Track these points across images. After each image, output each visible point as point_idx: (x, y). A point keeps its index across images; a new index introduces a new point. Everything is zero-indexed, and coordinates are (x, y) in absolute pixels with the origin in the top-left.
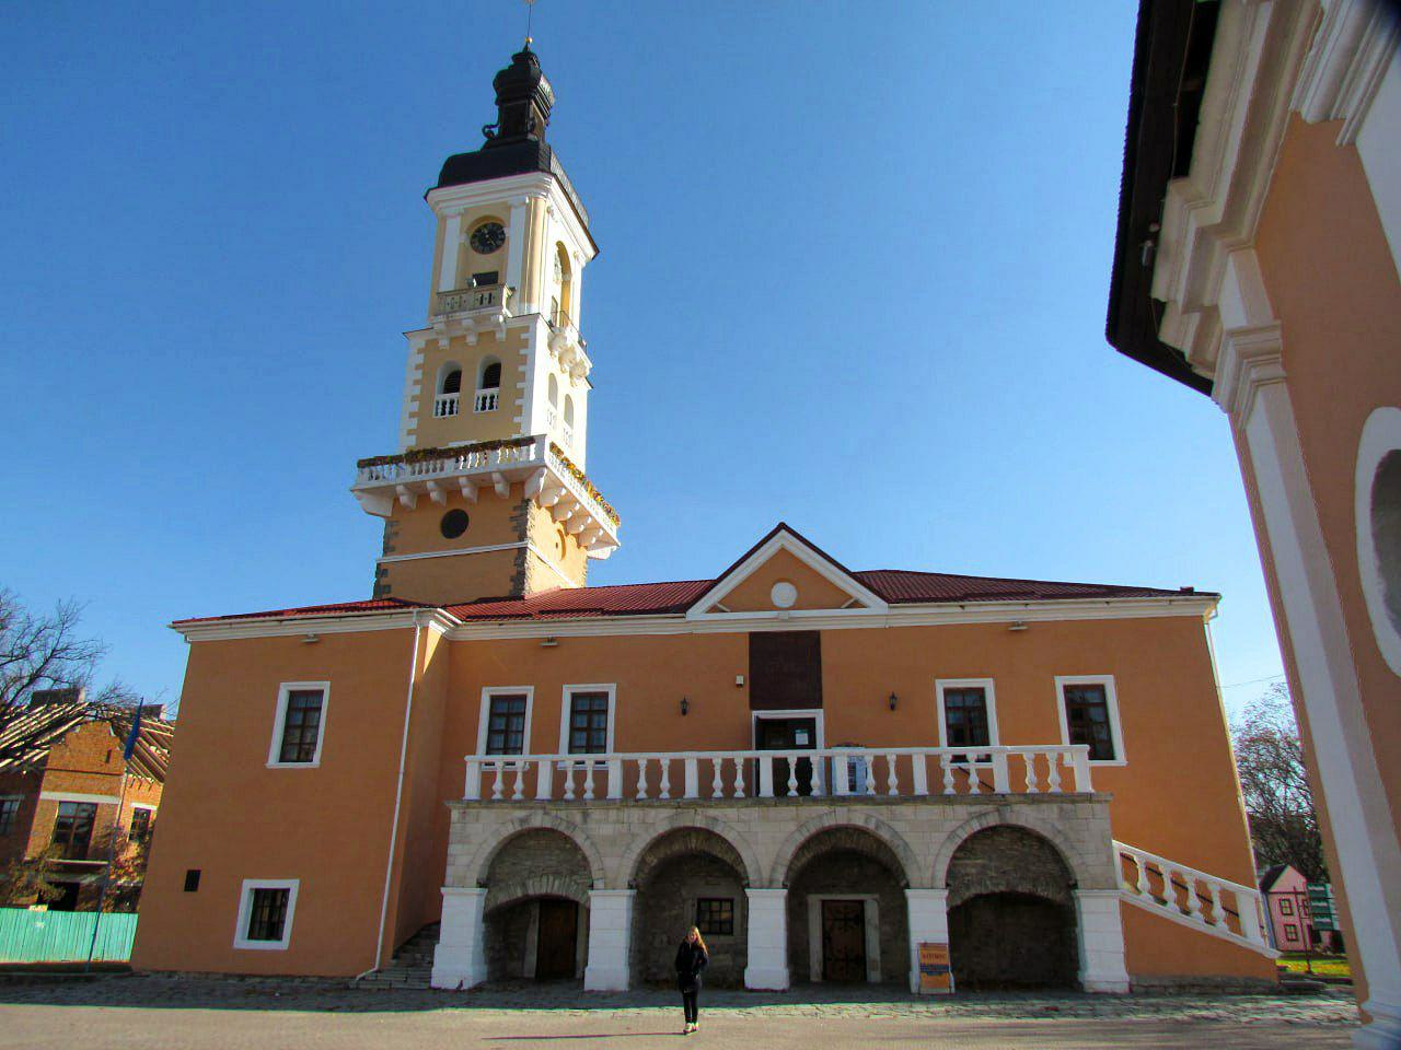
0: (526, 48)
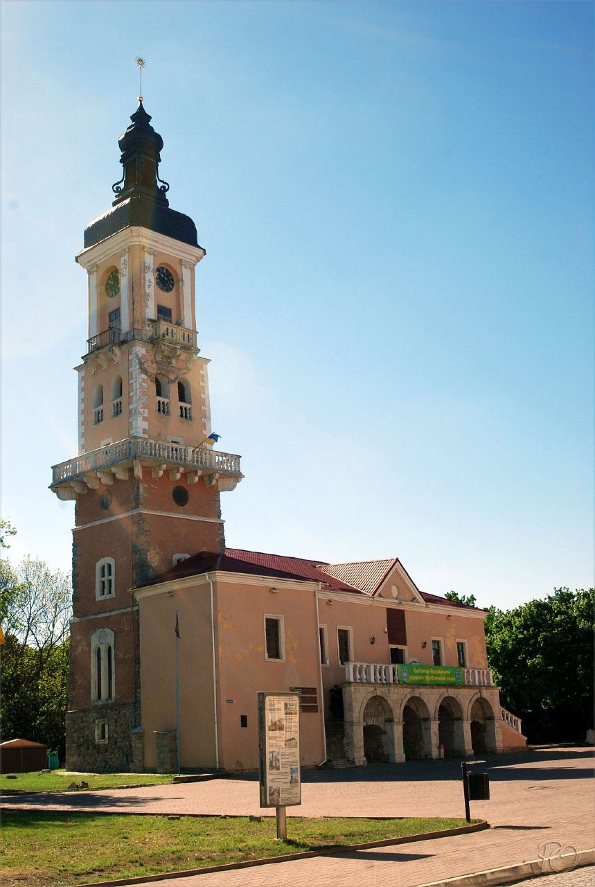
0: (141, 108)
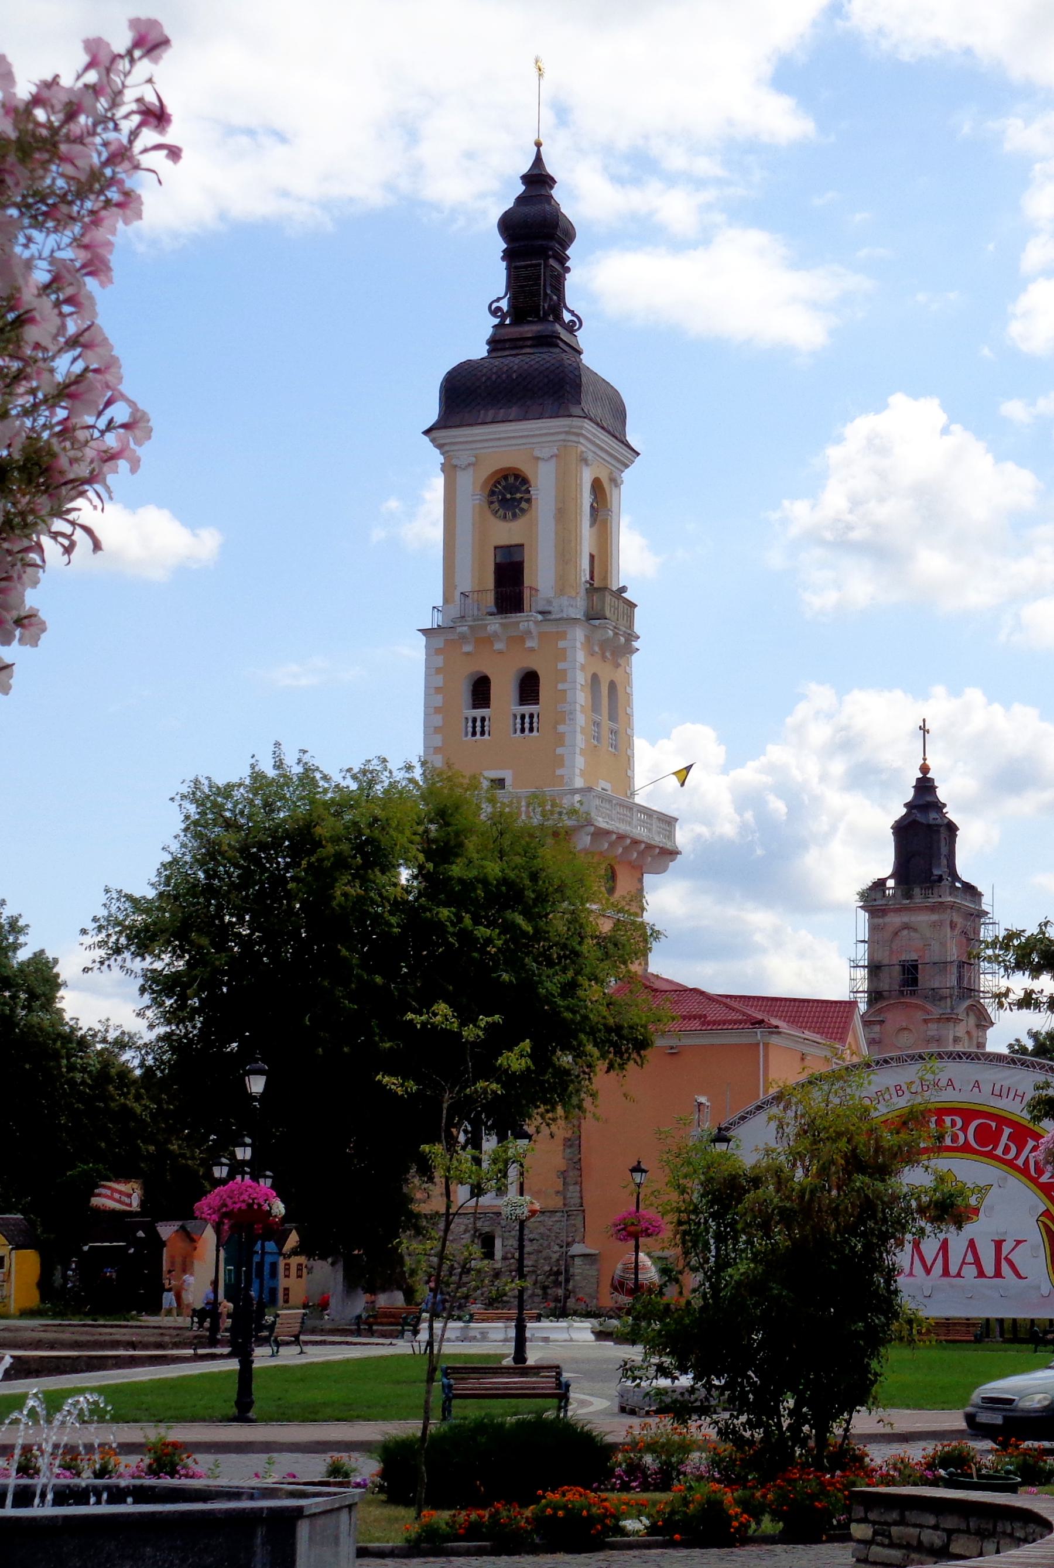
0: (538, 160)
